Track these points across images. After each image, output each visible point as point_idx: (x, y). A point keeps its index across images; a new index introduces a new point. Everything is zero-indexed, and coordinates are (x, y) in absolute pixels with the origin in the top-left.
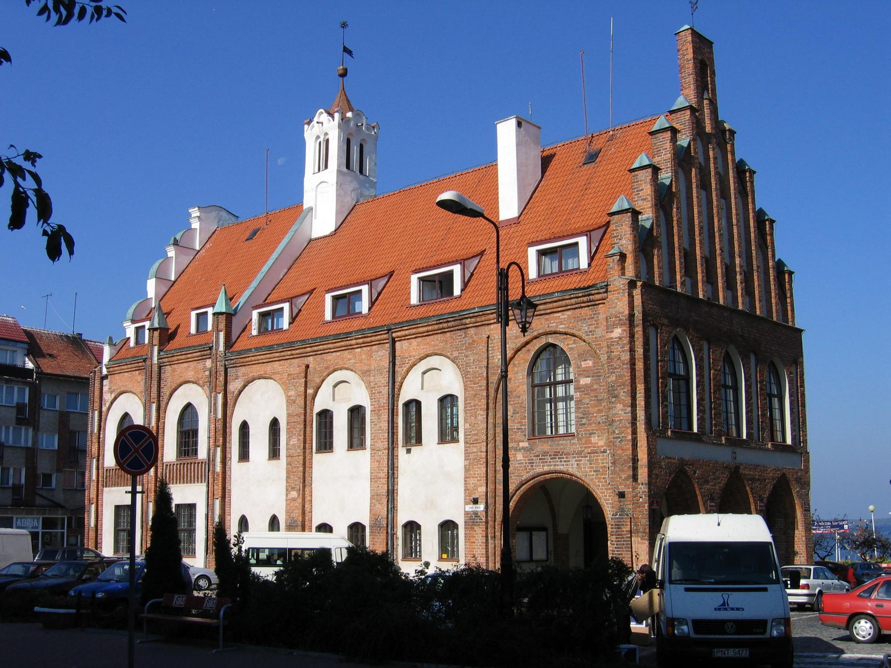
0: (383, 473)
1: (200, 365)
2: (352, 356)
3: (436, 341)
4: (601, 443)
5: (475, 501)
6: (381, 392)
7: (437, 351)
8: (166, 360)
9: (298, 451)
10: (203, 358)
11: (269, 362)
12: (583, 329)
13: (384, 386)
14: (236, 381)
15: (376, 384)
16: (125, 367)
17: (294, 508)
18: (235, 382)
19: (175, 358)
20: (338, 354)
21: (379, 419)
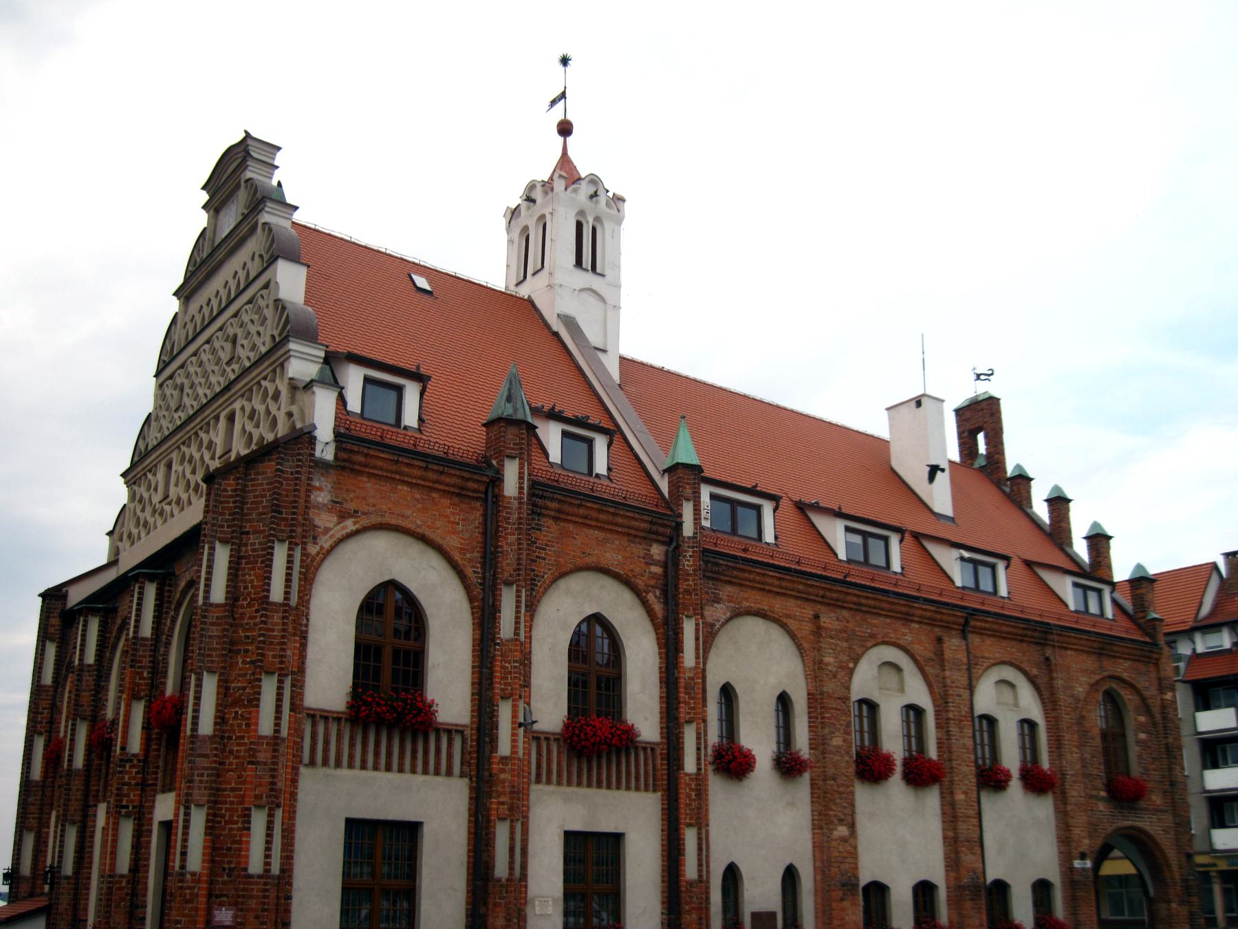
0: (974, 810)
1: (638, 549)
2: (907, 631)
3: (1013, 650)
4: (1159, 802)
5: (1083, 856)
6: (960, 696)
7: (1013, 661)
8: (555, 505)
9: (847, 758)
10: (649, 537)
11: (778, 593)
12: (1141, 683)
13: (964, 688)
14: (715, 605)
15: (953, 682)
16: (416, 472)
17: (845, 855)
18: (712, 606)
19: (582, 511)
20: (888, 620)
21: (961, 732)
